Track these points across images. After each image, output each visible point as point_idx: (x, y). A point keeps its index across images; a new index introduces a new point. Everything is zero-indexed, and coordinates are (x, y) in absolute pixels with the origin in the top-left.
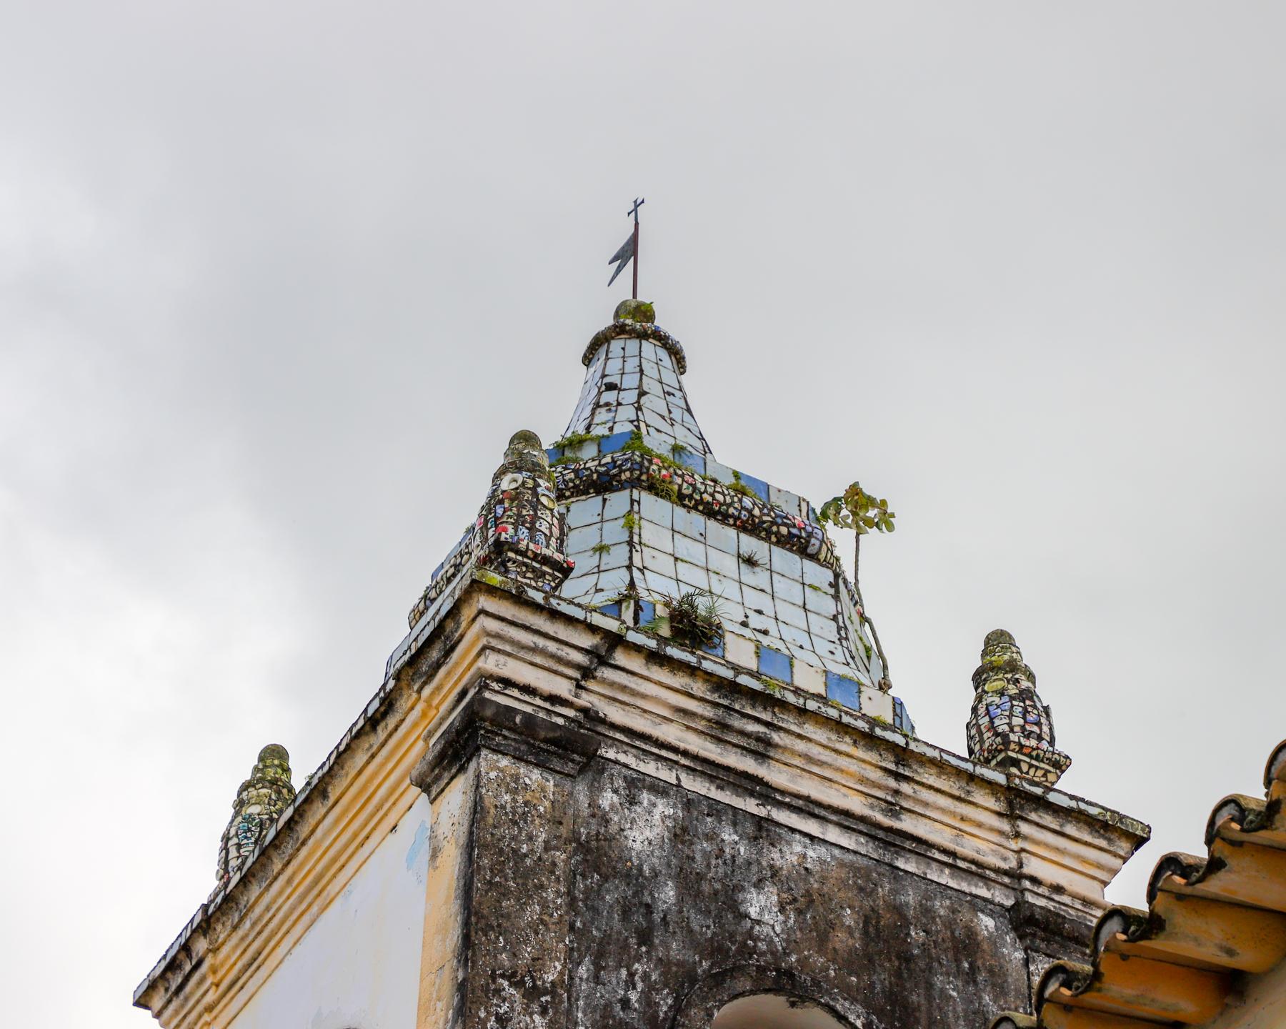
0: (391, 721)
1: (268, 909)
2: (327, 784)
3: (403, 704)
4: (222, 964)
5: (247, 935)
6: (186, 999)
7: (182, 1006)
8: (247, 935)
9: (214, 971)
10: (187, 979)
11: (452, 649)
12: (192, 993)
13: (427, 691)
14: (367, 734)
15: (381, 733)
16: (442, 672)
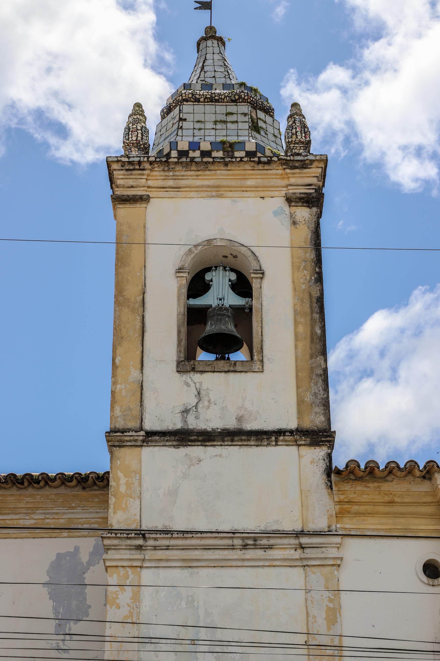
0: (266, 167)
1: (183, 176)
2: (229, 163)
3: (274, 166)
4: (152, 176)
5: (169, 176)
6: (131, 174)
7: (128, 175)
8: (169, 176)
9: (148, 175)
10: (134, 169)
11: (305, 168)
12: (135, 175)
13: (288, 171)
14: (255, 163)
15: (260, 167)
16: (297, 171)
